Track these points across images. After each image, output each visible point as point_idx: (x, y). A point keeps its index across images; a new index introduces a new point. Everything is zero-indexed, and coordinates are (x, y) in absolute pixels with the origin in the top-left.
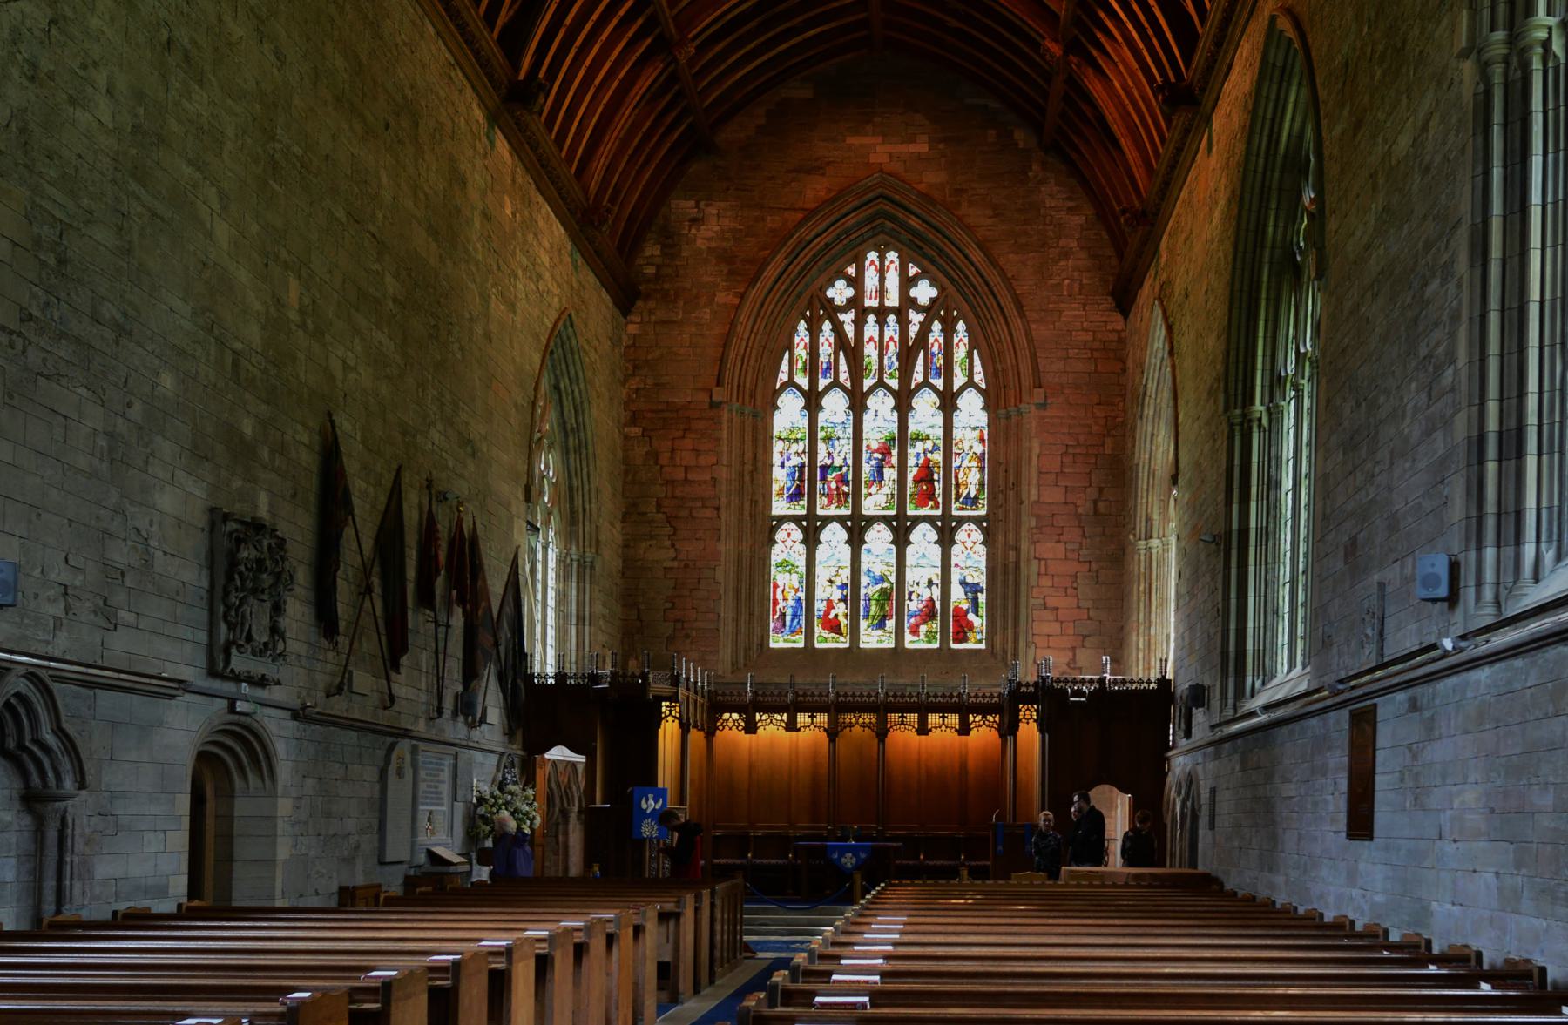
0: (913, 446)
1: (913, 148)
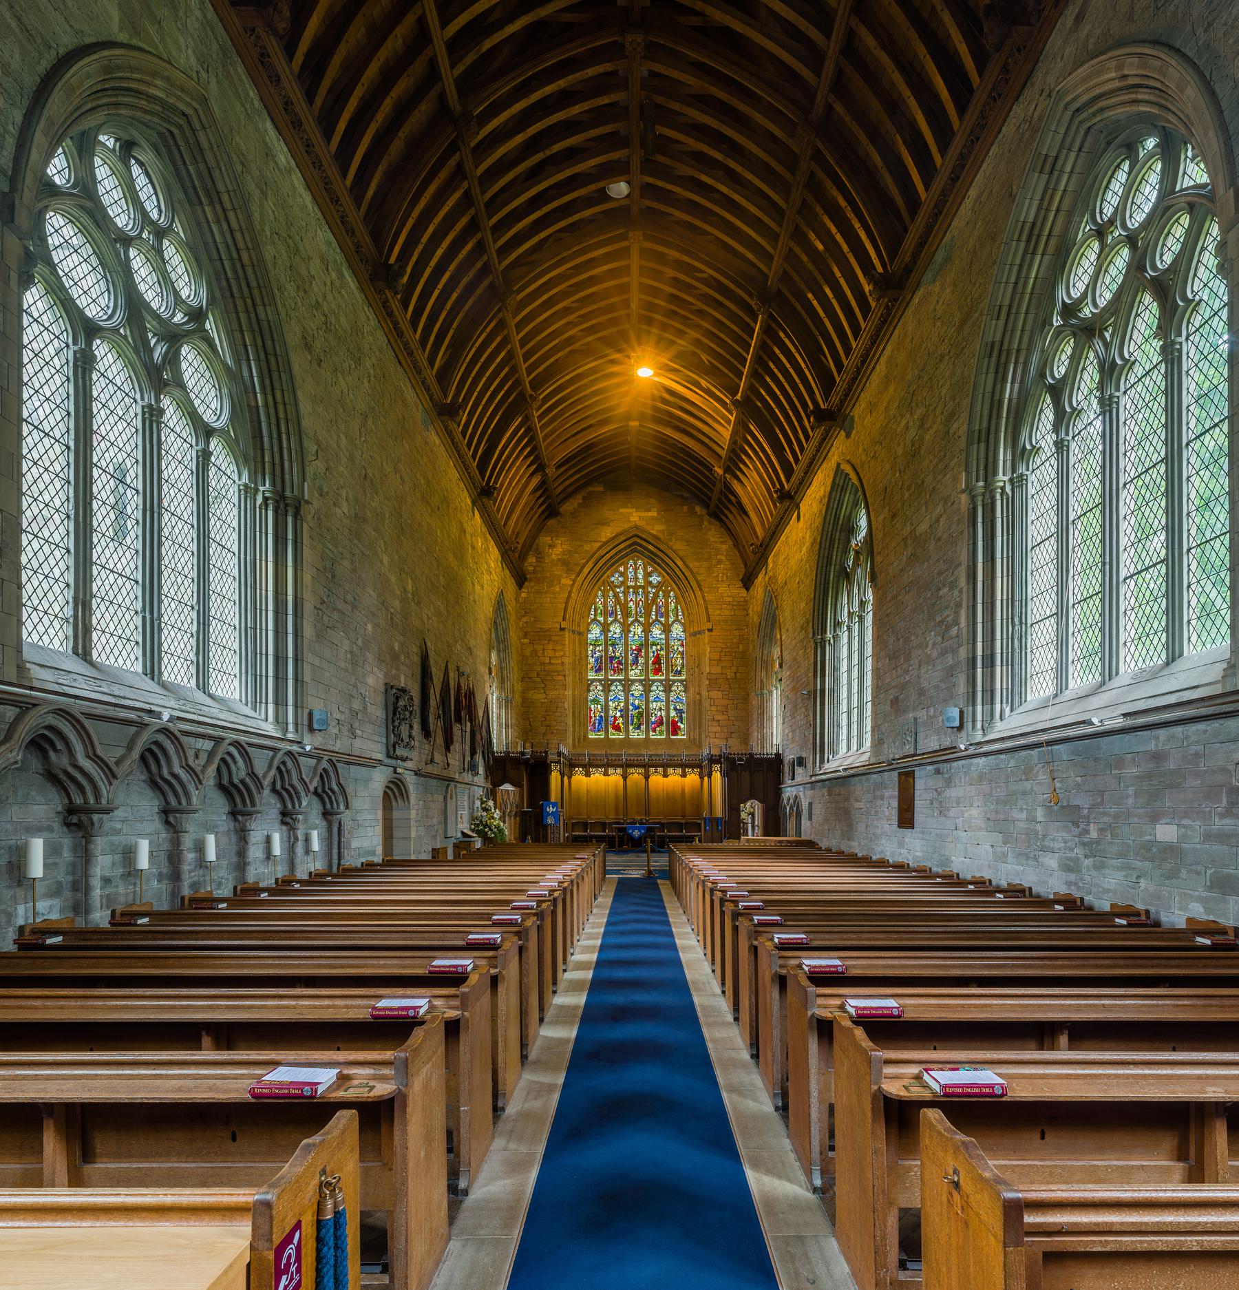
1: (650, 514)
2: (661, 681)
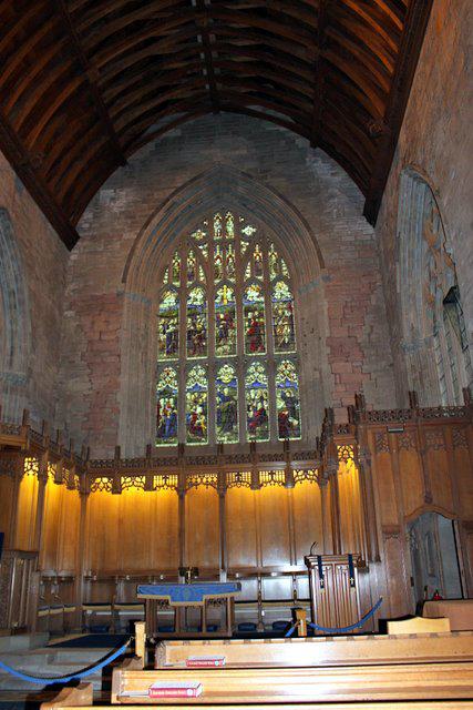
0: (247, 315)
2: (256, 359)
